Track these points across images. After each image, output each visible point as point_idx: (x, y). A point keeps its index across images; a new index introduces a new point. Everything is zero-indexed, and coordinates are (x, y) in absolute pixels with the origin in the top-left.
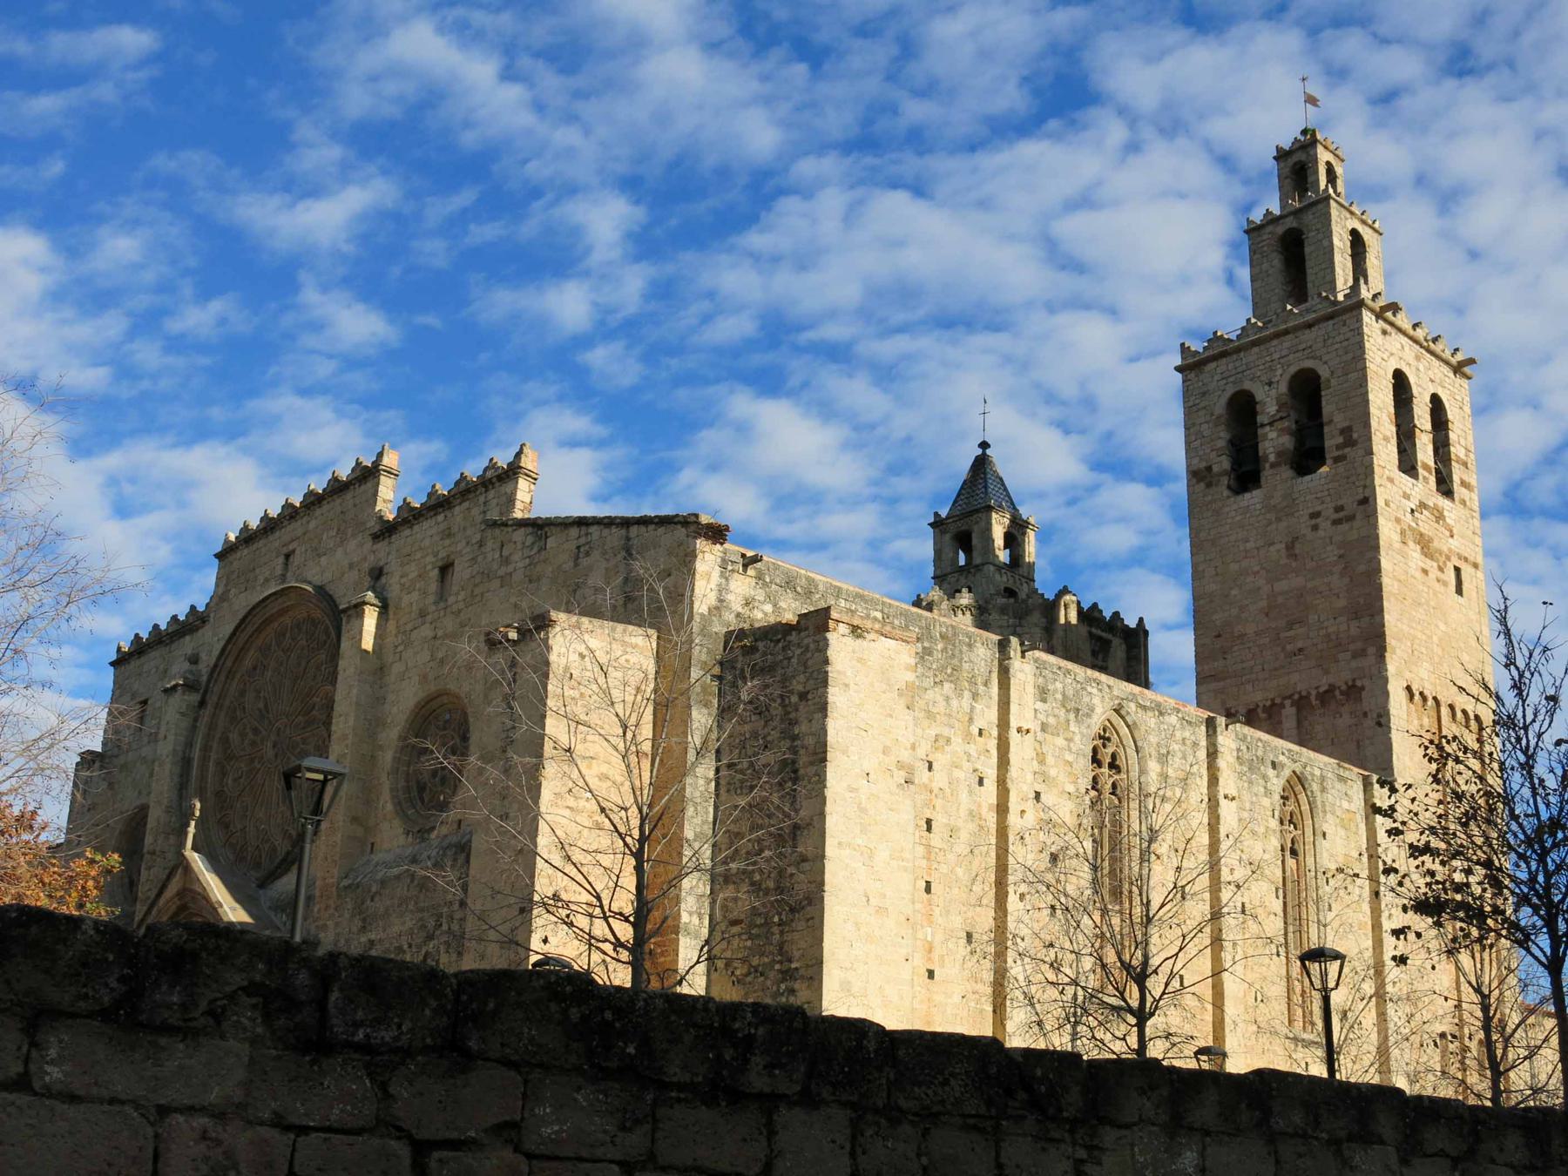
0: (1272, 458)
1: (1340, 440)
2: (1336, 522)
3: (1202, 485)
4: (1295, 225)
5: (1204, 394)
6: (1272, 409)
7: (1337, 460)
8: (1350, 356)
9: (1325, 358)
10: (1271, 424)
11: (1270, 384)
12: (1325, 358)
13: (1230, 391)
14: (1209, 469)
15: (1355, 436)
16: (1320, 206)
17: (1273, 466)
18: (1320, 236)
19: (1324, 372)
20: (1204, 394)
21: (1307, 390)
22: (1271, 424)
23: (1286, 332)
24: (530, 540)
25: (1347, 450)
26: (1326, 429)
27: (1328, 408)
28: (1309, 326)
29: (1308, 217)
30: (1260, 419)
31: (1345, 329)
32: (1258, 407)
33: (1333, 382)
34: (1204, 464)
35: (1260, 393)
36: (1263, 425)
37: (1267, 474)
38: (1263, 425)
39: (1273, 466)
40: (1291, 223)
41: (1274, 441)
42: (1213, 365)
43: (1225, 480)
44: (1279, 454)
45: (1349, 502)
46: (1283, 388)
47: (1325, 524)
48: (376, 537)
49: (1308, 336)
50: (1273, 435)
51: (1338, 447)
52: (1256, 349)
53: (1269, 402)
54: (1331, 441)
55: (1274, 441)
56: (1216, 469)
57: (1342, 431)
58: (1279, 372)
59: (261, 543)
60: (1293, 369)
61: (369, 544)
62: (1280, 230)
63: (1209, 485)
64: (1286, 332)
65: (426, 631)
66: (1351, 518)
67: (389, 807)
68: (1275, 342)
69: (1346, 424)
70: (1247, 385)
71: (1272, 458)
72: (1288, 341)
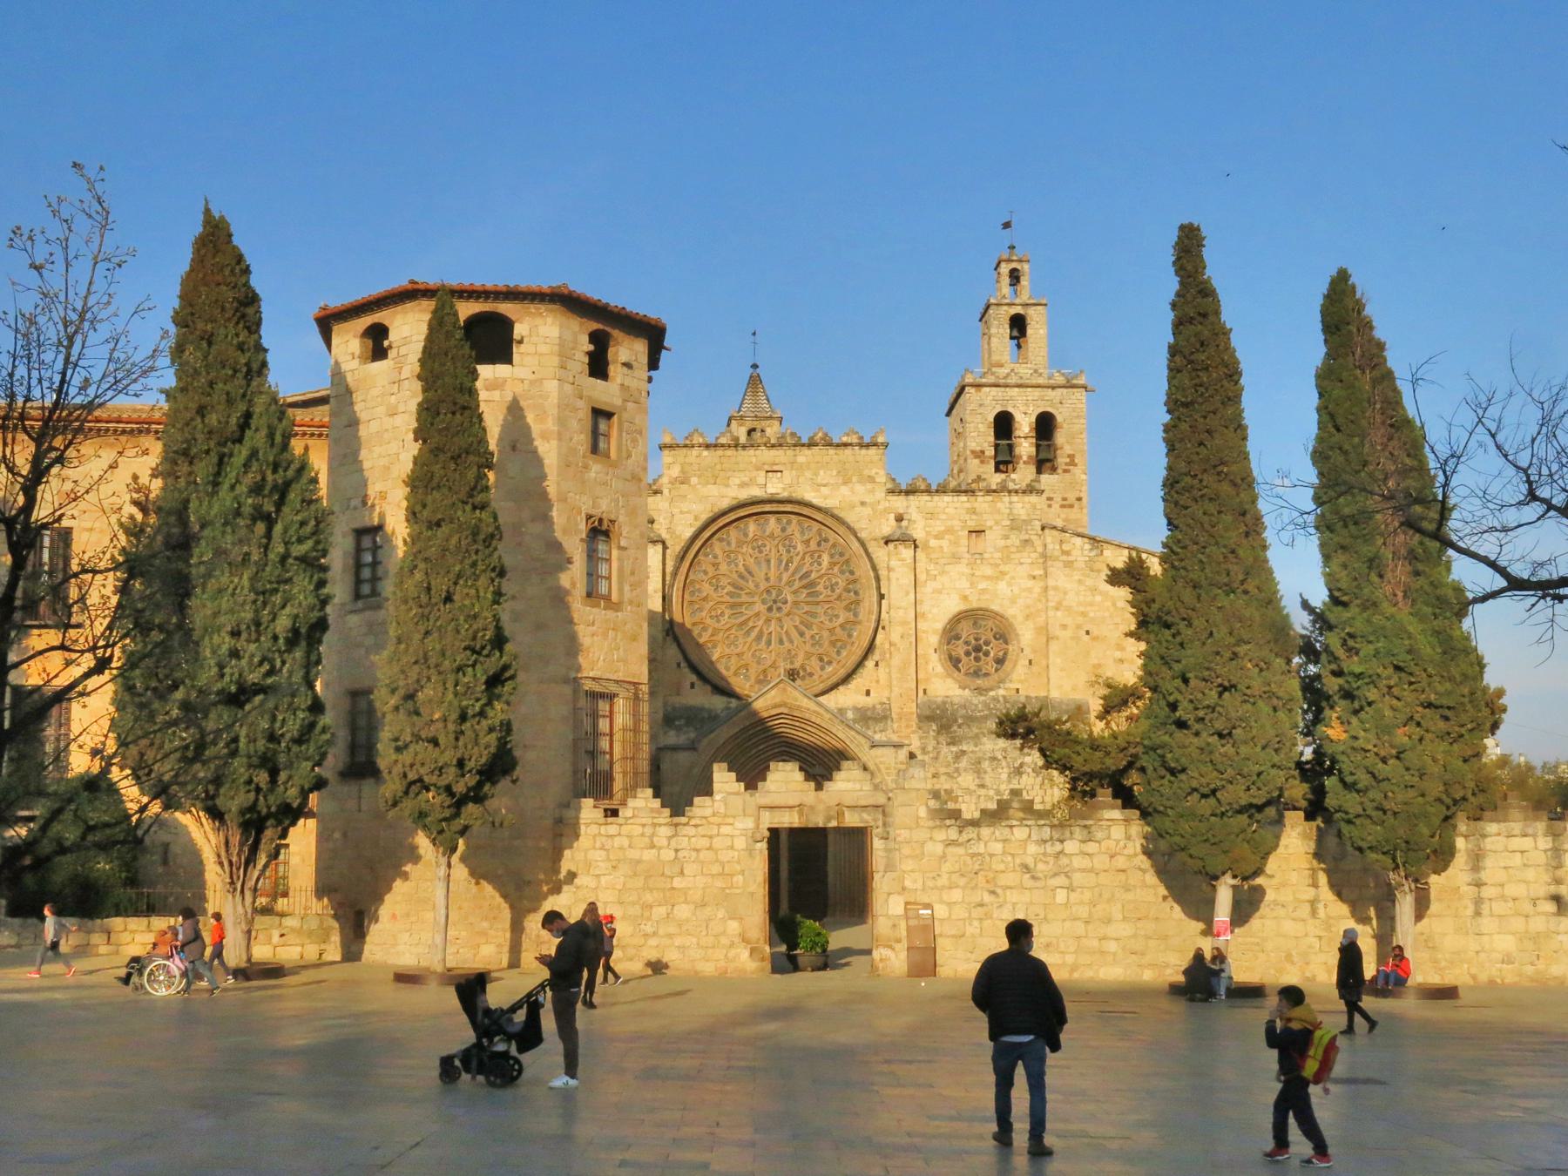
2: (1063, 506)
3: (977, 461)
7: (1065, 471)
13: (999, 409)
19: (1059, 419)
21: (1045, 426)
24: (1087, 546)
27: (1060, 438)
28: (1053, 388)
30: (1017, 433)
35: (1018, 416)
37: (1021, 465)
40: (1018, 310)
41: (1025, 447)
45: (1072, 497)
47: (1056, 506)
48: (891, 492)
53: (1024, 425)
54: (1061, 461)
55: (1025, 447)
59: (729, 452)
60: (1041, 410)
61: (880, 494)
65: (963, 568)
66: (1071, 506)
67: (939, 669)
70: (1010, 409)
72: (1037, 392)
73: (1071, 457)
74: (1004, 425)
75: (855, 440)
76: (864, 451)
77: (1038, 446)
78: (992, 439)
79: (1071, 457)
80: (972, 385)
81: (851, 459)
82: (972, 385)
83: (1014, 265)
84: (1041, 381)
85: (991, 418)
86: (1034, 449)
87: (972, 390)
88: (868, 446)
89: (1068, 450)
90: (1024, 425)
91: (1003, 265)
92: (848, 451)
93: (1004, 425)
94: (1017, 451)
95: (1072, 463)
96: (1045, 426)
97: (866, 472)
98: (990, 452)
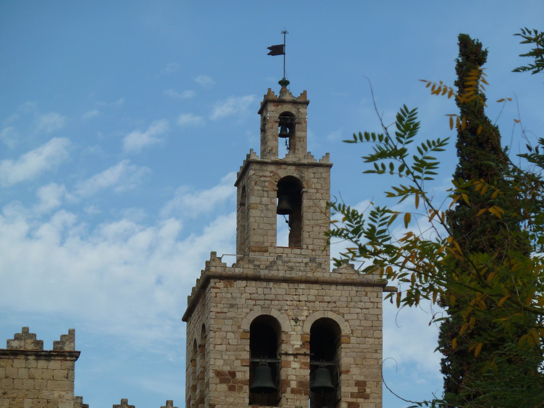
0: (294, 384)
1: (355, 390)
3: (224, 387)
4: (295, 175)
5: (232, 306)
6: (298, 343)
8: (368, 324)
9: (347, 317)
10: (295, 355)
11: (296, 320)
12: (347, 317)
13: (258, 312)
14: (233, 374)
15: (368, 391)
16: (321, 170)
17: (293, 391)
18: (318, 196)
19: (345, 329)
20: (232, 306)
22: (295, 355)
23: (316, 282)
25: (360, 400)
26: (343, 377)
27: (346, 357)
29: (308, 175)
30: (284, 348)
31: (366, 299)
32: (284, 337)
33: (353, 340)
34: (227, 369)
35: (286, 325)
36: (287, 354)
38: (287, 354)
39: (293, 391)
40: (291, 171)
42: (244, 283)
43: (246, 388)
44: (301, 383)
46: (307, 329)
49: (334, 292)
50: (296, 365)
51: (353, 395)
52: (284, 285)
53: (295, 337)
56: (239, 376)
57: (358, 384)
58: (306, 313)
60: (318, 316)
62: (283, 173)
63: (232, 389)
64: (316, 282)
68: (302, 286)
69: (361, 378)
70: (274, 313)
71: (294, 384)
72: (314, 291)
73: (361, 385)
74: (264, 335)
75: (30, 347)
76: (42, 363)
77: (313, 369)
78: (246, 355)
79: (361, 385)
80: (221, 277)
81: (23, 373)
82: (221, 277)
83: (287, 108)
84: (319, 275)
85: (246, 326)
86: (307, 372)
87: (221, 284)
88: (48, 356)
89: (356, 374)
90: (295, 337)
91: (271, 107)
92: (19, 362)
93: (264, 335)
94: (284, 373)
95: (362, 394)
96: (325, 339)
97: (46, 394)
98: (243, 374)
